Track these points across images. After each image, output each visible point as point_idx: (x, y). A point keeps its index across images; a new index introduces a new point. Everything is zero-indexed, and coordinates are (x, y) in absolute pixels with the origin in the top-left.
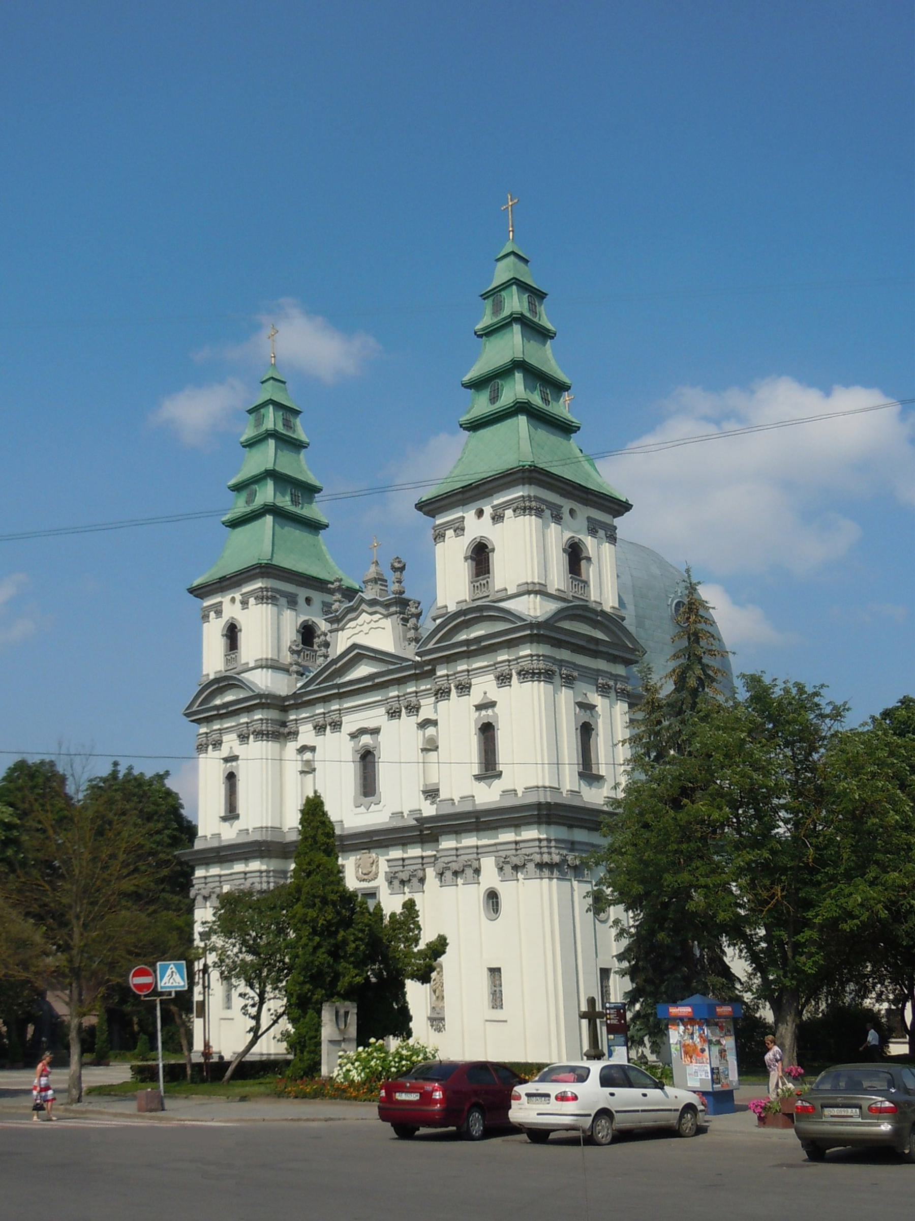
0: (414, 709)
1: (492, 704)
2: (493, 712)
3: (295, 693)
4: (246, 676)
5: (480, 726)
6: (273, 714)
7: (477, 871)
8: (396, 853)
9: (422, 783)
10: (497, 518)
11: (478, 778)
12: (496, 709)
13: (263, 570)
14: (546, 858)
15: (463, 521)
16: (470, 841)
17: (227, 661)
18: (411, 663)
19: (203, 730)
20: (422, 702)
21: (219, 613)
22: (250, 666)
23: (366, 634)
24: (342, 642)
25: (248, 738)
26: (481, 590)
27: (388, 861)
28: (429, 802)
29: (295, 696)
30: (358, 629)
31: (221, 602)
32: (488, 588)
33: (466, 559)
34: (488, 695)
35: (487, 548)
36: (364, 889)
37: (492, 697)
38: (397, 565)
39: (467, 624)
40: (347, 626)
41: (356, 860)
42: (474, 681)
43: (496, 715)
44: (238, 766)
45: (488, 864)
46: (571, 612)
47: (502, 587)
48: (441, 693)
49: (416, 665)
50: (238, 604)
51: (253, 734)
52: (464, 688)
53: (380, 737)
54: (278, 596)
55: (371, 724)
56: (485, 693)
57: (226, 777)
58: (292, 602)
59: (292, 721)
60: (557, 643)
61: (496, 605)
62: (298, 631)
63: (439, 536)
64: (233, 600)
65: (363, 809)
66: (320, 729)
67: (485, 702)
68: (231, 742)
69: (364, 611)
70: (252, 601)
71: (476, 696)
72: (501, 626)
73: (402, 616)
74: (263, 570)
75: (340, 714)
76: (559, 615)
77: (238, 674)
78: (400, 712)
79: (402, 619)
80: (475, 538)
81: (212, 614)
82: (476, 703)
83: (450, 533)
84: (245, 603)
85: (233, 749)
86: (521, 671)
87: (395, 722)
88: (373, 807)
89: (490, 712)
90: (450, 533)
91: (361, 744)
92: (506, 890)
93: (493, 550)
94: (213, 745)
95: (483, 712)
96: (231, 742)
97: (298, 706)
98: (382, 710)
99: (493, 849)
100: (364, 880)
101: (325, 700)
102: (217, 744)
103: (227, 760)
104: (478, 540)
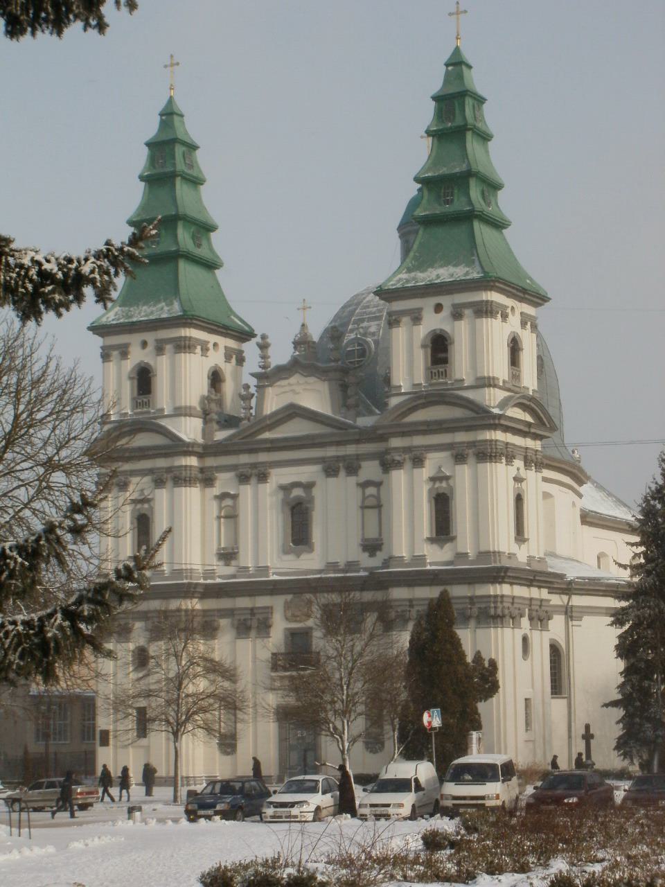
4: (163, 422)
5: (434, 496)
9: (360, 537)
10: (457, 315)
11: (431, 540)
12: (450, 481)
18: (357, 430)
20: (364, 464)
21: (124, 352)
24: (273, 401)
25: (165, 483)
26: (439, 376)
29: (220, 443)
30: (287, 389)
32: (446, 376)
36: (295, 629)
39: (424, 406)
40: (275, 385)
41: (286, 603)
43: (451, 489)
44: (152, 509)
47: (458, 376)
52: (418, 462)
53: (316, 492)
55: (304, 479)
58: (205, 350)
60: (506, 429)
62: (208, 377)
63: (393, 321)
64: (144, 344)
65: (291, 557)
66: (243, 479)
67: (441, 475)
69: (296, 372)
70: (169, 347)
72: (457, 413)
73: (341, 382)
77: (155, 418)
79: (341, 386)
80: (435, 330)
81: (115, 353)
84: (160, 350)
86: (479, 453)
87: (332, 480)
88: (304, 556)
89: (444, 484)
93: (452, 343)
95: (437, 485)
100: (296, 621)
103: (134, 502)
104: (438, 332)
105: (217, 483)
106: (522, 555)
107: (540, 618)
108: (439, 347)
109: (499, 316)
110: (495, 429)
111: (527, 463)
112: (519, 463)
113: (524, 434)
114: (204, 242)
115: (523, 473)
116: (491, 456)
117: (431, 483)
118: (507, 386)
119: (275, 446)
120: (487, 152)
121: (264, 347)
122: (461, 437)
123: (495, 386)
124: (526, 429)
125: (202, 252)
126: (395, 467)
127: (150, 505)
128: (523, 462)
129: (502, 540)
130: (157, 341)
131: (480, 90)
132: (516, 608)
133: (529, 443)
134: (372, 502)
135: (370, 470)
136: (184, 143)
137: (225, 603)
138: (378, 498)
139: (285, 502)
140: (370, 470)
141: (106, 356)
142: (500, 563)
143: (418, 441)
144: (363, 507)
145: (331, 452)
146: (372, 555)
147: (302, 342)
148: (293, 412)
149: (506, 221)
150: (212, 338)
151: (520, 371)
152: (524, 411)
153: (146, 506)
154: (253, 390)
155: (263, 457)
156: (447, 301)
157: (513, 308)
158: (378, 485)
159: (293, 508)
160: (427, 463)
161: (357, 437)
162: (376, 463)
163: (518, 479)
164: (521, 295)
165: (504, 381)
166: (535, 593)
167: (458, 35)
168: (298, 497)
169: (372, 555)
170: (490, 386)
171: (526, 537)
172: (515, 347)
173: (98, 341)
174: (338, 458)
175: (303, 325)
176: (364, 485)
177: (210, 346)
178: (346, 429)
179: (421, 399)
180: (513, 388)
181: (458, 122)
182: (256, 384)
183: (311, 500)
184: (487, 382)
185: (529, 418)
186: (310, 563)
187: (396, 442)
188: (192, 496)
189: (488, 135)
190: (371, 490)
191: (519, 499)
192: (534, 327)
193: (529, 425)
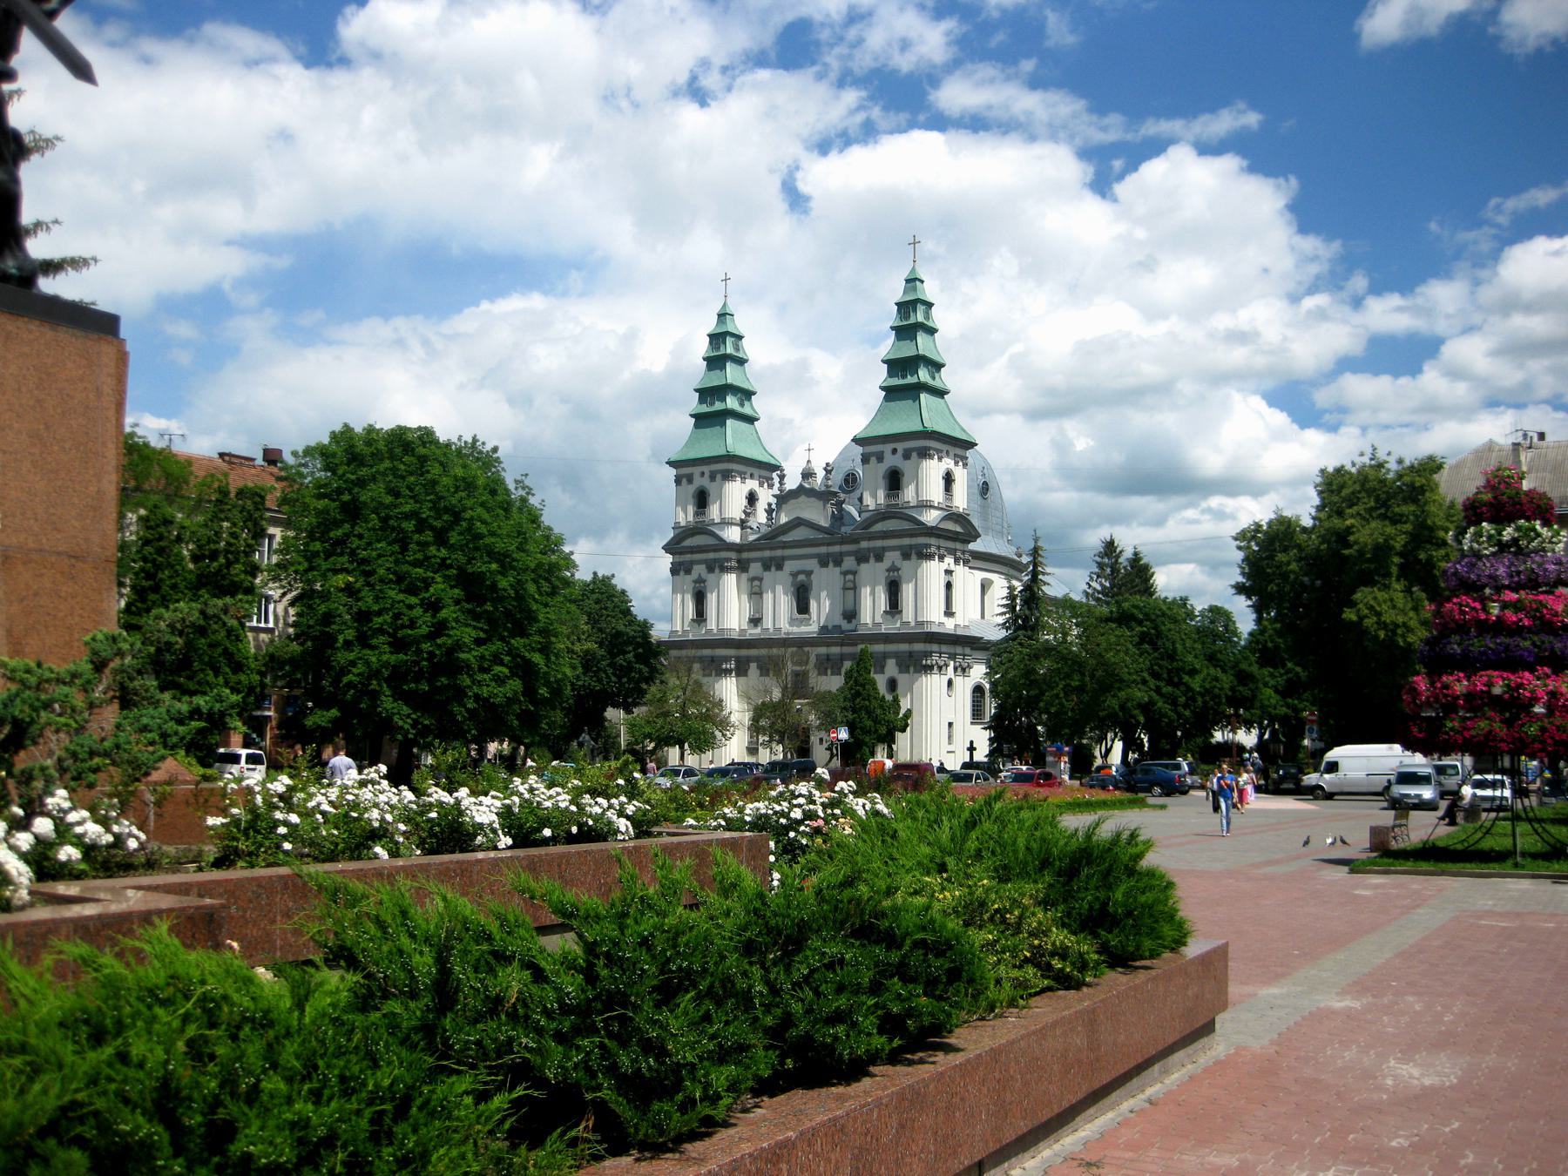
1: (898, 570)
6: (733, 555)
7: (883, 667)
8: (823, 650)
10: (907, 456)
16: (879, 648)
17: (696, 514)
19: (679, 558)
21: (690, 479)
37: (898, 563)
42: (887, 554)
43: (900, 577)
49: (842, 537)
52: (879, 558)
55: (808, 568)
60: (939, 536)
64: (703, 474)
66: (767, 567)
68: (699, 570)
70: (719, 477)
71: (887, 563)
72: (906, 525)
81: (684, 480)
83: (873, 460)
84: (713, 478)
90: (873, 460)
92: (902, 679)
96: (699, 570)
99: (896, 655)
101: (771, 549)
102: (688, 572)
103: (695, 582)
106: (949, 625)
107: (963, 670)
108: (894, 481)
111: (957, 561)
112: (949, 560)
114: (746, 403)
115: (952, 567)
119: (785, 546)
121: (782, 477)
122: (907, 541)
123: (932, 507)
125: (747, 410)
129: (934, 615)
131: (930, 299)
133: (958, 546)
134: (850, 585)
135: (849, 562)
136: (733, 335)
137: (753, 652)
138: (854, 582)
139: (793, 584)
140: (849, 562)
141: (678, 481)
143: (879, 543)
144: (845, 589)
145: (823, 550)
146: (850, 622)
147: (807, 474)
148: (797, 523)
150: (750, 470)
154: (774, 506)
155: (779, 553)
156: (900, 446)
157: (947, 452)
158: (854, 573)
159: (798, 589)
163: (949, 572)
166: (959, 650)
169: (850, 622)
172: (949, 479)
173: (673, 472)
174: (828, 555)
176: (845, 573)
177: (748, 476)
179: (881, 515)
181: (912, 320)
183: (811, 583)
184: (927, 505)
185: (959, 529)
186: (811, 628)
187: (864, 544)
188: (730, 580)
190: (850, 577)
191: (949, 586)
192: (965, 465)
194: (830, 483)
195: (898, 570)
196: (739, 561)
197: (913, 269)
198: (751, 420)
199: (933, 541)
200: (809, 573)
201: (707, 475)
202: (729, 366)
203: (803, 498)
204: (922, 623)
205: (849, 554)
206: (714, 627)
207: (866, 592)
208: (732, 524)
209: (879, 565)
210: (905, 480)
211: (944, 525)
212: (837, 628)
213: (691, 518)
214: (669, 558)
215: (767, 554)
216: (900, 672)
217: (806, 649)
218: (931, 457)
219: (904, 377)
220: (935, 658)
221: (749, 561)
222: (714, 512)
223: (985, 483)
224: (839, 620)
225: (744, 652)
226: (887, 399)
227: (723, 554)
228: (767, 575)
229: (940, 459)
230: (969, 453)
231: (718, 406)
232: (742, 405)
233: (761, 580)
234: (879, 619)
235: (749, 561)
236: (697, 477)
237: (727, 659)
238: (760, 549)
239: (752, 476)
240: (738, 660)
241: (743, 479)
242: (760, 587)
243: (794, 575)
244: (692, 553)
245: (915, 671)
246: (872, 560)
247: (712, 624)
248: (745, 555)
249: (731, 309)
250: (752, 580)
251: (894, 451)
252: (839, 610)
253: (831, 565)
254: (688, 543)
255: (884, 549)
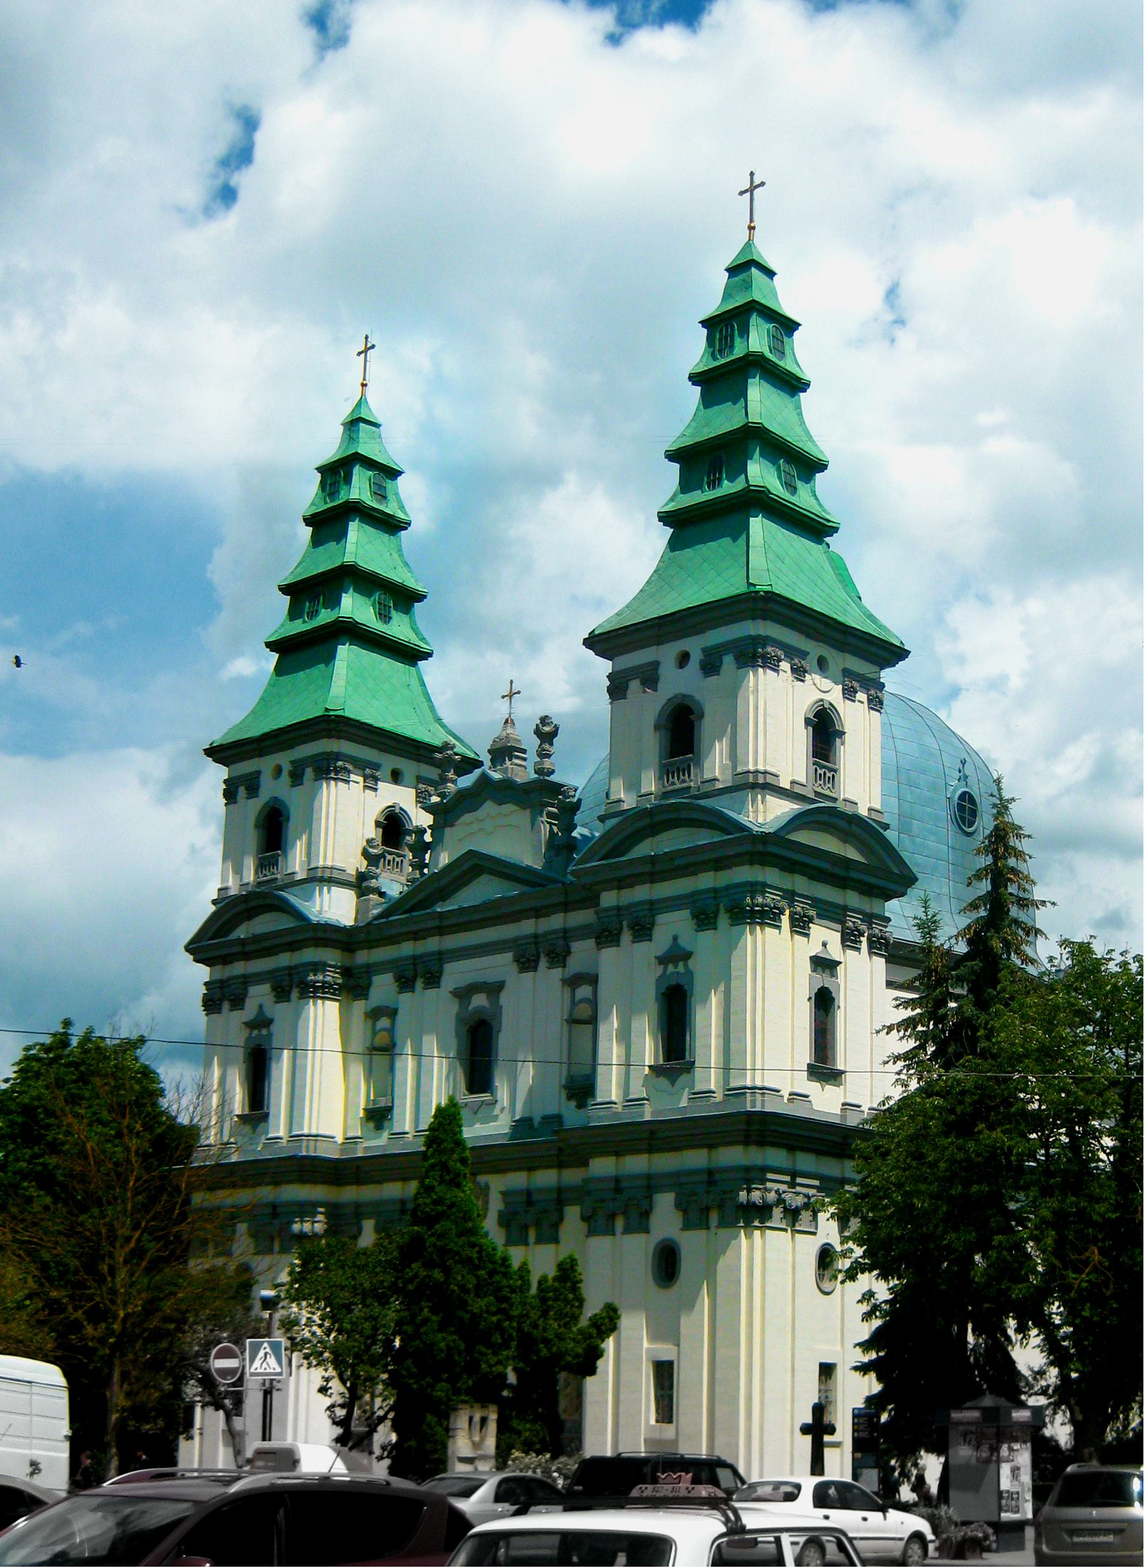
0: (559, 957)
1: (687, 956)
2: (686, 966)
3: (369, 924)
6: (332, 956)
7: (646, 1214)
8: (517, 1180)
9: (565, 1073)
10: (711, 666)
12: (691, 962)
13: (333, 725)
14: (756, 1196)
15: (657, 669)
16: (637, 1164)
18: (560, 885)
22: (298, 877)
23: (488, 834)
27: (503, 1193)
28: (573, 1104)
31: (258, 773)
33: (657, 727)
34: (682, 942)
35: (693, 713)
38: (547, 729)
40: (459, 821)
42: (661, 919)
43: (690, 974)
45: (665, 1203)
46: (813, 818)
48: (607, 936)
50: (285, 777)
51: (298, 986)
53: (504, 998)
54: (350, 767)
55: (492, 977)
56: (675, 938)
57: (249, 1054)
59: (362, 966)
60: (790, 866)
61: (702, 802)
64: (278, 771)
66: (405, 983)
68: (260, 995)
71: (661, 940)
72: (704, 838)
74: (333, 725)
75: (440, 960)
76: (797, 822)
78: (537, 961)
81: (242, 791)
82: (659, 954)
83: (635, 685)
85: (265, 1009)
89: (681, 968)
90: (635, 685)
91: (470, 1008)
93: (702, 716)
94: (230, 1000)
95: (671, 968)
96: (260, 995)
97: (371, 944)
98: (508, 957)
99: (676, 1181)
101: (416, 936)
105: (373, 992)
109: (785, 666)
110: (763, 864)
111: (850, 939)
113: (842, 883)
115: (835, 951)
116: (752, 911)
117: (660, 970)
118: (798, 789)
120: (798, 407)
122: (706, 880)
124: (841, 872)
126: (606, 942)
127: (269, 1030)
128: (839, 935)
130: (291, 762)
131: (789, 310)
132: (798, 1194)
133: (852, 899)
134: (584, 1011)
136: (369, 463)
139: (460, 1019)
141: (230, 795)
142: (763, 1106)
143: (641, 893)
144: (573, 1021)
149: (829, 521)
150: (390, 762)
151: (835, 771)
152: (845, 842)
153: (264, 1032)
155: (432, 944)
156: (695, 645)
160: (657, 933)
161: (562, 899)
162: (591, 943)
163: (823, 964)
164: (840, 637)
165: (793, 782)
167: (751, 221)
168: (479, 1010)
169: (581, 1105)
170: (754, 786)
171: (840, 1066)
175: (506, 722)
176: (573, 982)
178: (544, 886)
180: (812, 796)
182: (431, 823)
183: (498, 1010)
184: (764, 785)
185: (852, 854)
187: (609, 899)
189: (799, 379)
191: (824, 1001)
192: (876, 703)
193: (847, 863)
194: (547, 763)
195: (687, 956)
196: (346, 972)
197: (749, 245)
198: (411, 655)
199: (771, 875)
200: (495, 989)
201: (287, 768)
202: (356, 530)
203: (489, 807)
204: (740, 1092)
205: (582, 932)
206: (282, 1133)
207: (610, 1026)
208: (332, 881)
209: (643, 947)
210: (707, 726)
211: (804, 837)
212: (554, 1121)
213: (250, 876)
214: (203, 973)
215: (407, 949)
216: (687, 1226)
217: (482, 1179)
218: (772, 664)
219: (714, 483)
220: (774, 1187)
221: (370, 970)
222: (296, 862)
223: (966, 797)
224: (555, 1103)
225: (350, 1194)
226: (674, 544)
227: (310, 955)
228: (405, 1001)
229: (799, 673)
230: (888, 676)
231: (325, 616)
232: (385, 617)
233: (392, 1013)
234: (638, 1090)
235: (370, 970)
236: (266, 781)
237: (305, 1209)
238: (393, 940)
239: (396, 777)
240: (334, 1212)
241: (371, 781)
242: (391, 1031)
243: (463, 994)
244: (247, 956)
245: (725, 1223)
246: (626, 937)
247: (279, 1128)
248: (363, 957)
249: (376, 408)
250: (374, 1014)
251: (684, 659)
252: (557, 1076)
253: (543, 963)
254: (242, 932)
255: (654, 907)
